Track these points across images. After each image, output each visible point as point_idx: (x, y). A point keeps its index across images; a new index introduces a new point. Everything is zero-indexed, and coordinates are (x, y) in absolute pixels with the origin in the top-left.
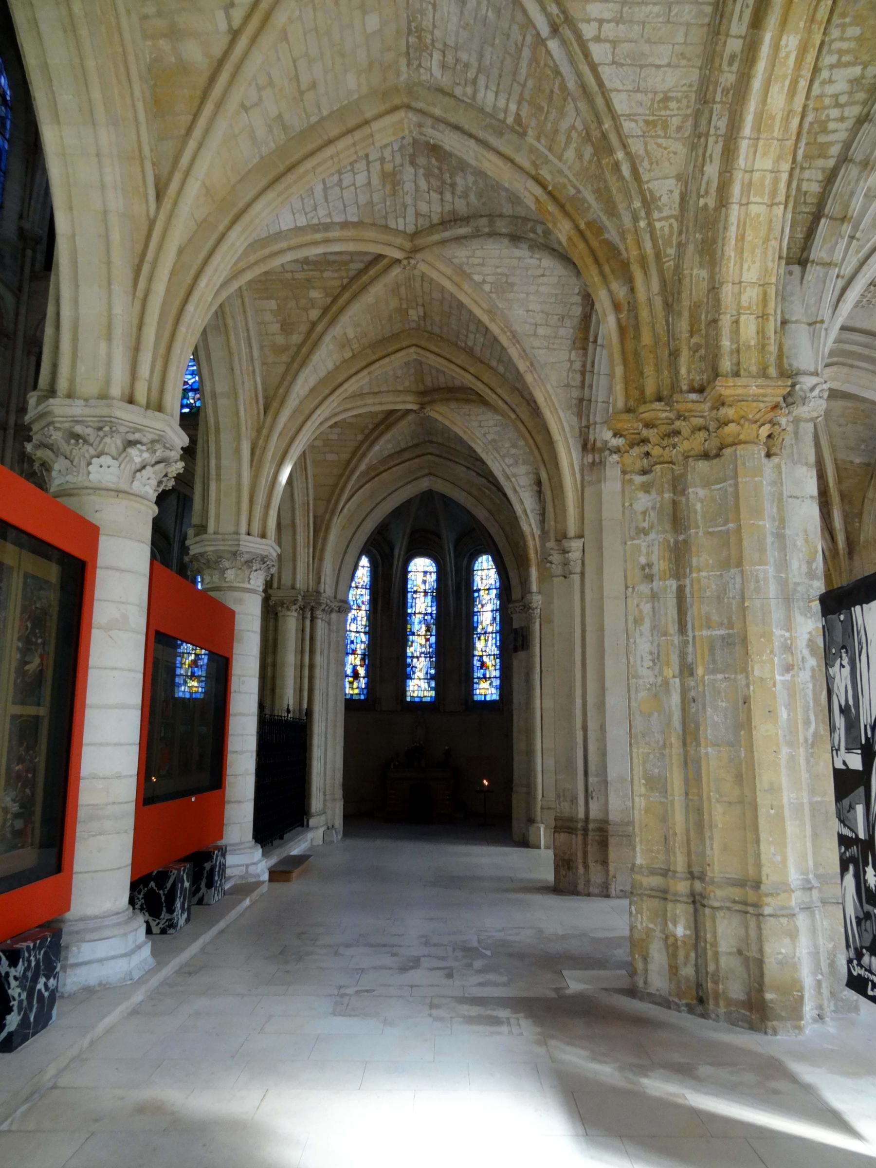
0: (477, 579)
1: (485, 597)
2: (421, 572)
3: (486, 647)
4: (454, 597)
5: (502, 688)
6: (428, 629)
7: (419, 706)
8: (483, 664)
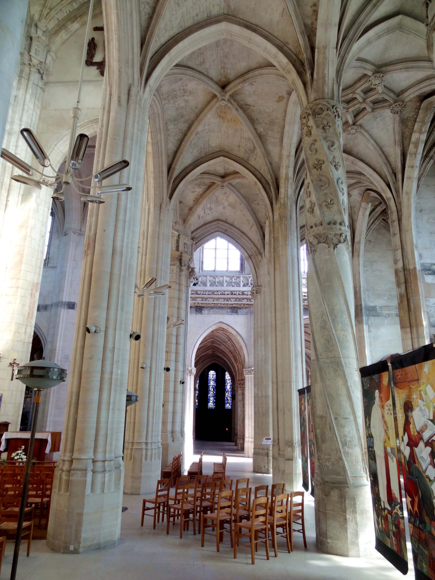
0: (226, 377)
1: (228, 382)
2: (212, 374)
3: (228, 395)
4: (220, 381)
5: (231, 406)
6: (214, 390)
7: (211, 409)
8: (228, 399)
